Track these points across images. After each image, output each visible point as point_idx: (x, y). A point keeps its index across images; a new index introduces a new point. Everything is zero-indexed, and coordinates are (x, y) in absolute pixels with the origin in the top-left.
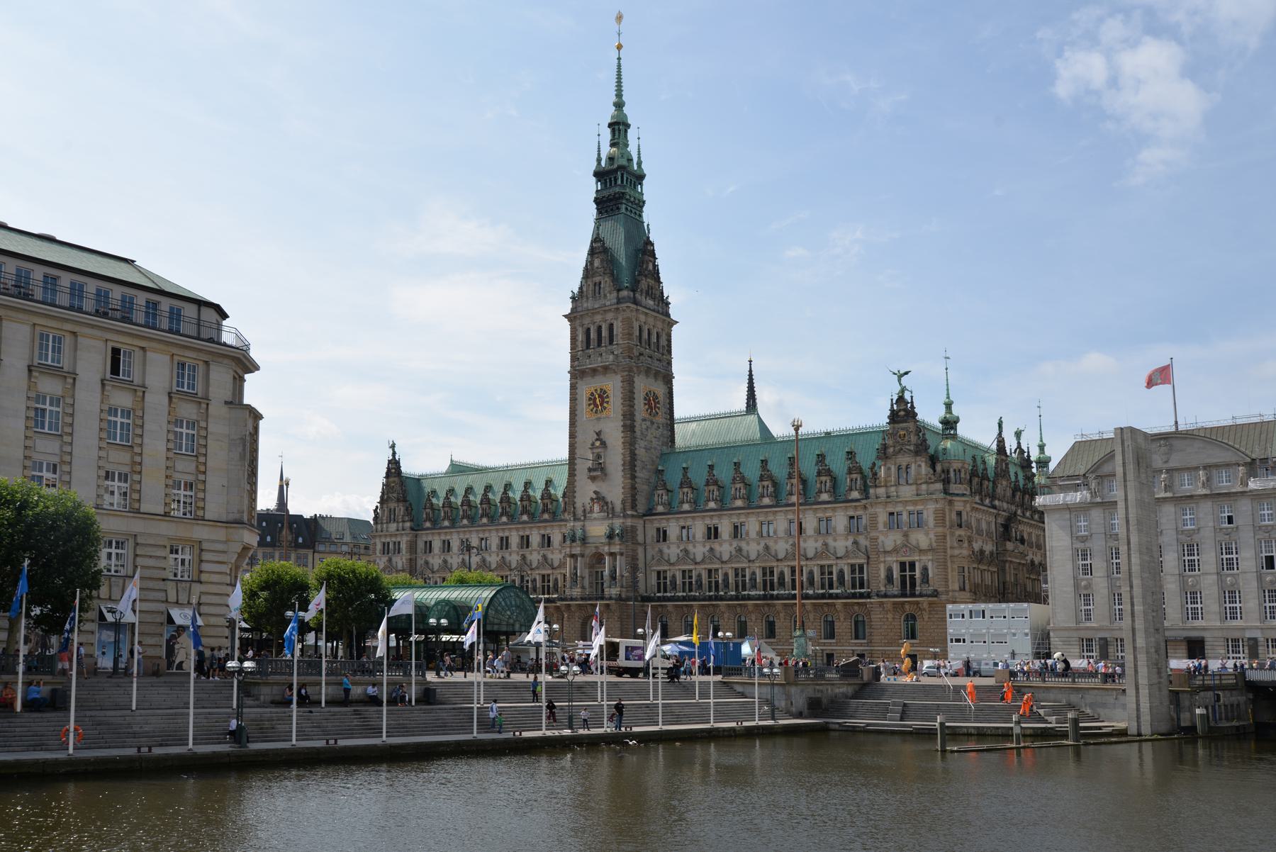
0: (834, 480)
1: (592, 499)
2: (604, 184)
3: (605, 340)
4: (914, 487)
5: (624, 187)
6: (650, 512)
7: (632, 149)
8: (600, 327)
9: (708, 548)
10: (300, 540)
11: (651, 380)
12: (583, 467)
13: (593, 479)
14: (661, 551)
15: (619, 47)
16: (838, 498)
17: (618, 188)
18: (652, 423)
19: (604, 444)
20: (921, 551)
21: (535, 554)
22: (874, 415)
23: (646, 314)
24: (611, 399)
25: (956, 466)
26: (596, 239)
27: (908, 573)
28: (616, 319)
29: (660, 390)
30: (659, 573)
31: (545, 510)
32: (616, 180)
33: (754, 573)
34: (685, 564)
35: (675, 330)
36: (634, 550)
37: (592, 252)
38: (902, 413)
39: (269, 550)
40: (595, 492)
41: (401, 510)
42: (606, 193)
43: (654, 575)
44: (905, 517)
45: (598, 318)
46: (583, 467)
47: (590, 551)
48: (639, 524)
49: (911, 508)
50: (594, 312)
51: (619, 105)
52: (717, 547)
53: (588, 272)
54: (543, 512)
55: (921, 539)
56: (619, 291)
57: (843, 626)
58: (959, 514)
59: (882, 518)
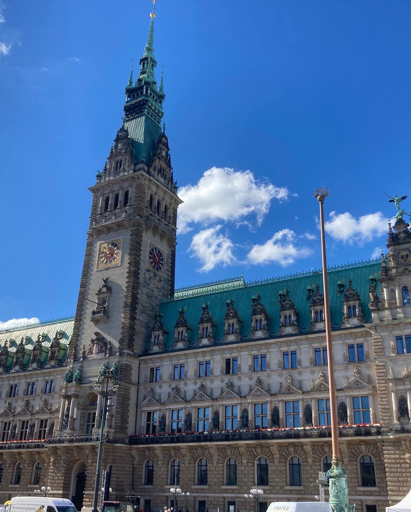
1: (93, 341)
5: (147, 96)
6: (146, 352)
11: (157, 239)
18: (155, 275)
23: (158, 186)
29: (164, 248)
30: (149, 414)
32: (142, 93)
34: (176, 402)
36: (127, 390)
40: (97, 334)
43: (144, 416)
48: (134, 363)
52: (208, 384)
56: (135, 165)
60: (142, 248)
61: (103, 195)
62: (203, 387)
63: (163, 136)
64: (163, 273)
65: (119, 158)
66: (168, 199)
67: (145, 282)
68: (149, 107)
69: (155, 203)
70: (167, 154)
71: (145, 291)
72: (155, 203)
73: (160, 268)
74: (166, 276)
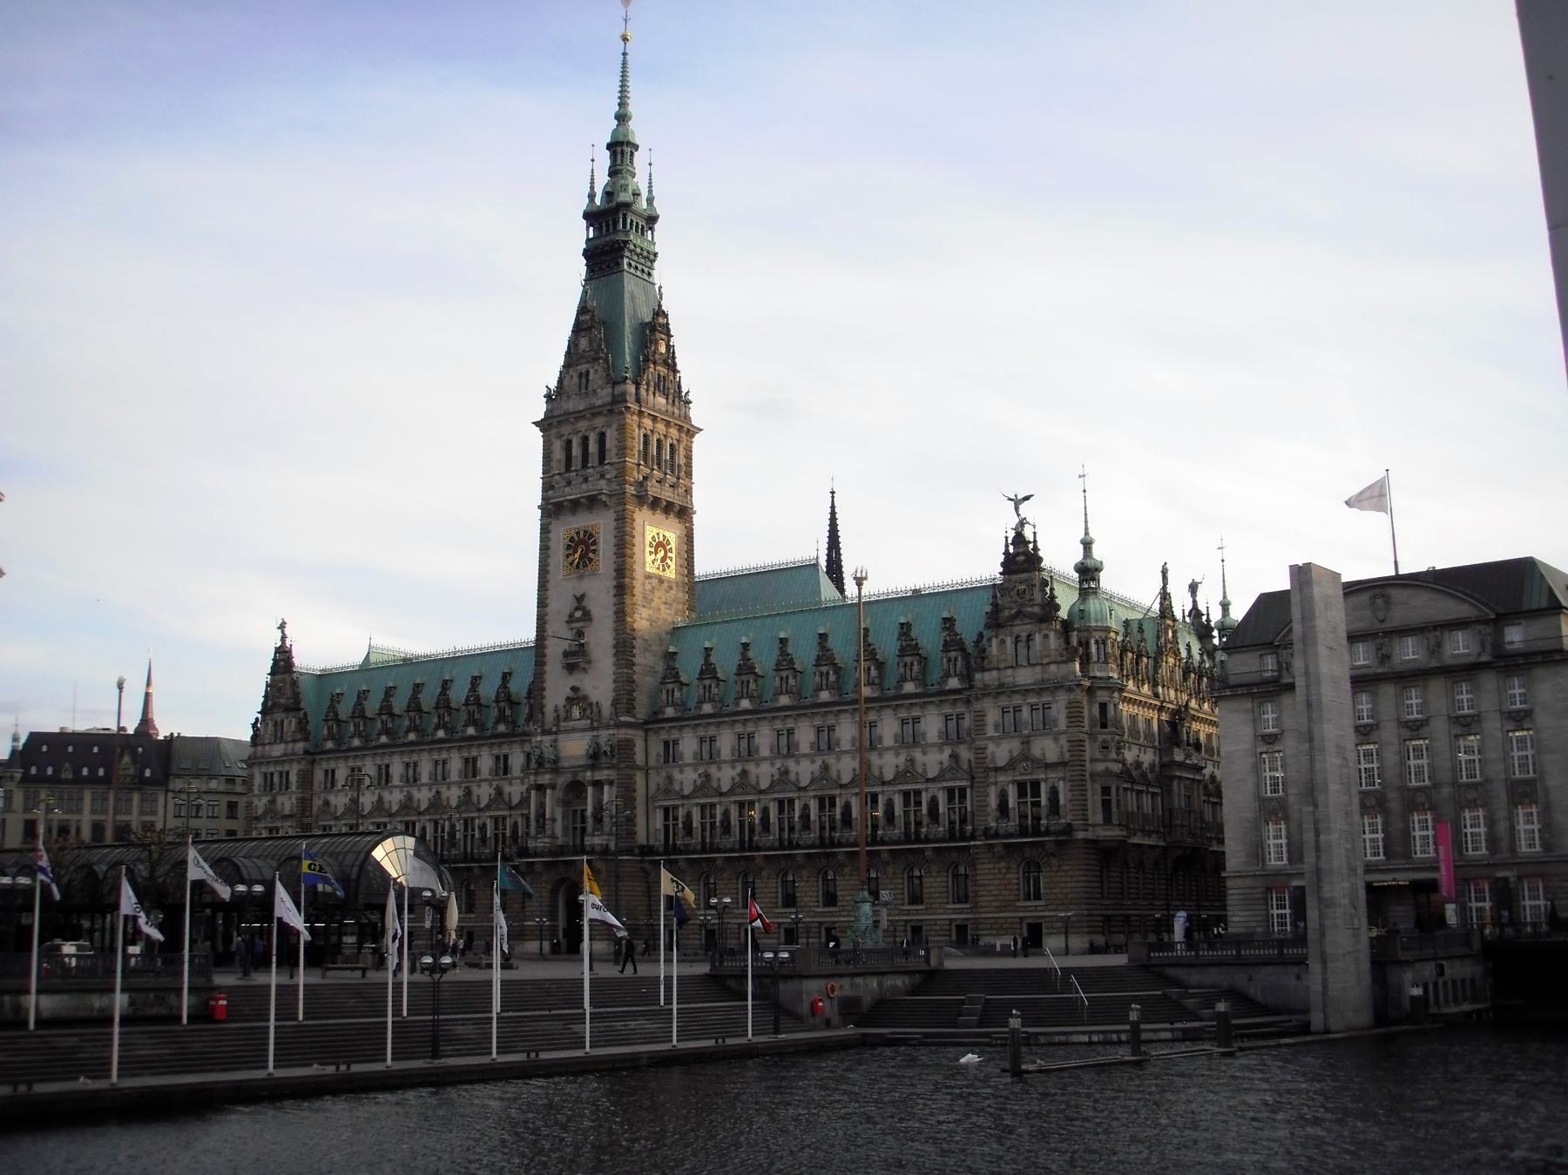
0: (924, 661)
1: (568, 699)
2: (598, 230)
3: (593, 460)
4: (1038, 669)
7: (640, 181)
8: (585, 440)
9: (739, 769)
10: (148, 773)
11: (659, 516)
12: (555, 650)
13: (571, 668)
14: (670, 779)
16: (933, 695)
17: (615, 235)
18: (661, 580)
19: (587, 616)
20: (1049, 766)
21: (485, 786)
22: (983, 564)
23: (654, 419)
24: (601, 546)
25: (1097, 635)
26: (583, 310)
27: (1029, 799)
28: (609, 426)
30: (666, 810)
31: (502, 718)
32: (615, 223)
33: (806, 807)
34: (706, 796)
36: (631, 777)
37: (579, 328)
38: (1021, 558)
39: (101, 789)
40: (574, 689)
41: (291, 724)
42: (597, 242)
43: (659, 815)
44: (1025, 713)
45: (582, 425)
46: (555, 650)
47: (562, 780)
48: (638, 736)
49: (1033, 700)
50: (578, 416)
51: (622, 118)
53: (573, 357)
54: (498, 722)
55: (1047, 748)
56: (615, 384)
57: (936, 883)
58: (1103, 707)
60: (637, 541)
61: (560, 436)
62: (744, 773)
63: (659, 313)
65: (583, 368)
66: (674, 432)
70: (668, 347)
74: (680, 578)
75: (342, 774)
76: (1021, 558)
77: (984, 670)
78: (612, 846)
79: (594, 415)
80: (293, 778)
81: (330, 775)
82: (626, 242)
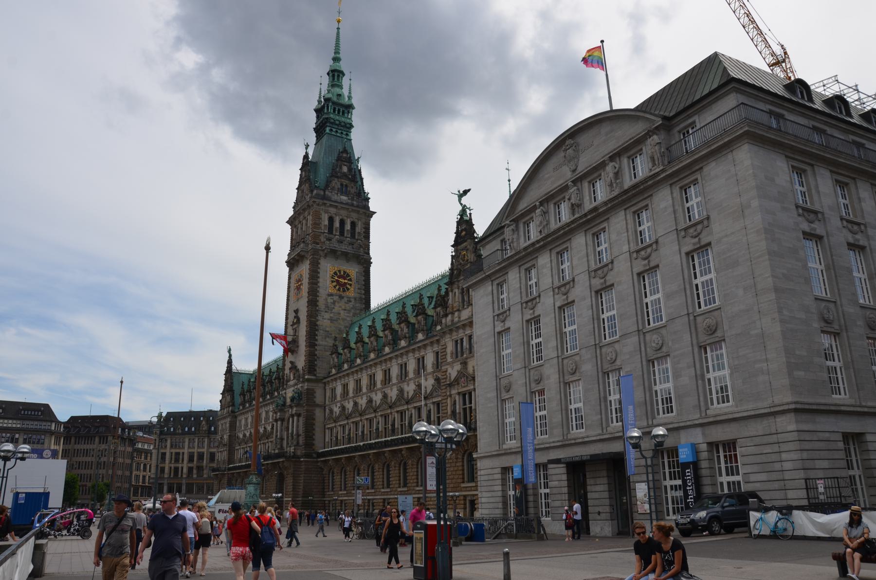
1: (290, 369)
15: (339, 22)
23: (336, 207)
35: (373, 221)
38: (464, 233)
39: (192, 437)
40: (291, 362)
47: (287, 415)
49: (468, 332)
56: (312, 191)
59: (450, 348)
64: (352, 293)
66: (354, 216)
67: (327, 306)
68: (332, 123)
69: (337, 224)
71: (327, 316)
72: (337, 224)
73: (348, 289)
74: (357, 295)
75: (243, 422)
76: (464, 233)
77: (446, 315)
78: (299, 453)
79: (304, 210)
80: (228, 425)
81: (240, 421)
82: (327, 118)
